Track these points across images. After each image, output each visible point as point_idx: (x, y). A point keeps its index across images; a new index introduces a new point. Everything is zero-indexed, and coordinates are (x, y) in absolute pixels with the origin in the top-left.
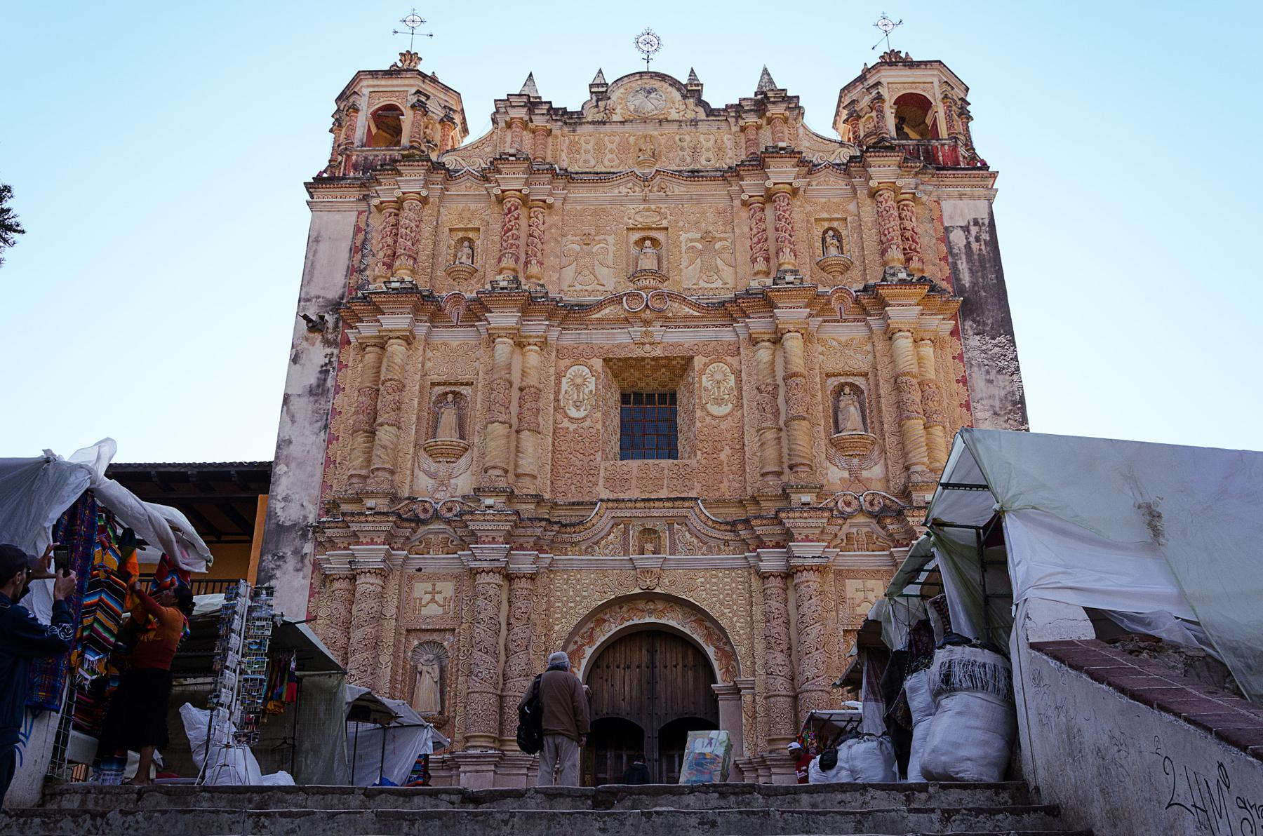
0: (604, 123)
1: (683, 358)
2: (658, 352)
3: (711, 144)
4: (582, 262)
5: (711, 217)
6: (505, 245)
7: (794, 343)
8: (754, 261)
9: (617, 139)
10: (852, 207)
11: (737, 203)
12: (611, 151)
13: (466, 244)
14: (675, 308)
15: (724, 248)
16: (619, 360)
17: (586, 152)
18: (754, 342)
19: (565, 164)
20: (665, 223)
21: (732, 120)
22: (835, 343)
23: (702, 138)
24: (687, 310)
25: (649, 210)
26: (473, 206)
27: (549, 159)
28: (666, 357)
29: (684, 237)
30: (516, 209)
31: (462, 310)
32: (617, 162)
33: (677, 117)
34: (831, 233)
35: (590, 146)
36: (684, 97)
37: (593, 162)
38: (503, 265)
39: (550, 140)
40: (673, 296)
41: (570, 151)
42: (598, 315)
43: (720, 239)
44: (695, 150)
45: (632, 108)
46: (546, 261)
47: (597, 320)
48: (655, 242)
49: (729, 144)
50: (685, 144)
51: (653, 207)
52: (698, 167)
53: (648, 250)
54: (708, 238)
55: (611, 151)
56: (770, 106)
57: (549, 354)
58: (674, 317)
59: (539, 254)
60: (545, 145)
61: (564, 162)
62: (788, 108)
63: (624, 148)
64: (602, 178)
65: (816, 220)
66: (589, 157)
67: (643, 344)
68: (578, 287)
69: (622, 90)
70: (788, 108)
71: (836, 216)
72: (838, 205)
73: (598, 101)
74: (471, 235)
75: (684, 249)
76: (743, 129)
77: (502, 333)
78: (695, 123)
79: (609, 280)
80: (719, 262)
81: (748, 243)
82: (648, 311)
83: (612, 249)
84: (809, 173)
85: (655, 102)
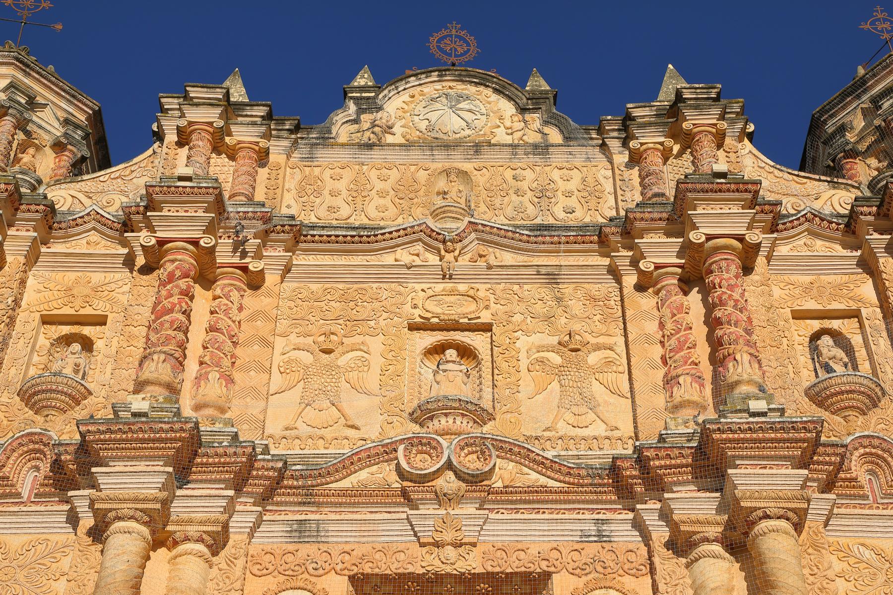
0: (369, 146)
1: (526, 577)
2: (473, 563)
3: (573, 185)
4: (316, 383)
5: (576, 307)
6: (153, 337)
7: (776, 542)
8: (670, 381)
9: (394, 174)
10: (867, 290)
11: (630, 280)
12: (382, 194)
13: (76, 347)
14: (506, 472)
15: (609, 362)
16: (385, 578)
17: (334, 194)
18: (682, 545)
19: (293, 211)
20: (485, 317)
21: (614, 145)
22: (868, 554)
23: (556, 175)
24: (534, 477)
25: (452, 293)
26: (97, 278)
27: (259, 196)
28: (489, 577)
29: (523, 342)
30: (186, 276)
31: (45, 467)
32: (392, 211)
33: (508, 140)
34: (826, 341)
35: (342, 185)
36: (523, 110)
37: (345, 211)
38: (146, 375)
39: (263, 172)
40: (509, 449)
41: (301, 192)
42: (345, 484)
43: (598, 348)
44: (543, 194)
45: (423, 125)
46: (237, 376)
47: (344, 493)
48: (466, 352)
49: (608, 186)
50: (524, 185)
51: (462, 288)
52: (551, 221)
53: (450, 366)
54: (571, 346)
55: (382, 194)
56: (687, 113)
57: (230, 562)
58: (507, 490)
59: (226, 362)
60: (253, 176)
61: (289, 205)
62: (722, 117)
63: (405, 192)
64: (363, 238)
65: (799, 315)
66: (338, 202)
67: (437, 545)
68: (303, 430)
69: (405, 97)
70: (722, 117)
71: (835, 306)
72: (840, 287)
73: (360, 111)
74: (87, 331)
75: (524, 364)
76: (635, 159)
77: (126, 508)
78: (542, 149)
79: (374, 421)
80: (596, 387)
81: (657, 352)
82: (450, 475)
83: (377, 362)
84: (773, 229)
85: (468, 116)
